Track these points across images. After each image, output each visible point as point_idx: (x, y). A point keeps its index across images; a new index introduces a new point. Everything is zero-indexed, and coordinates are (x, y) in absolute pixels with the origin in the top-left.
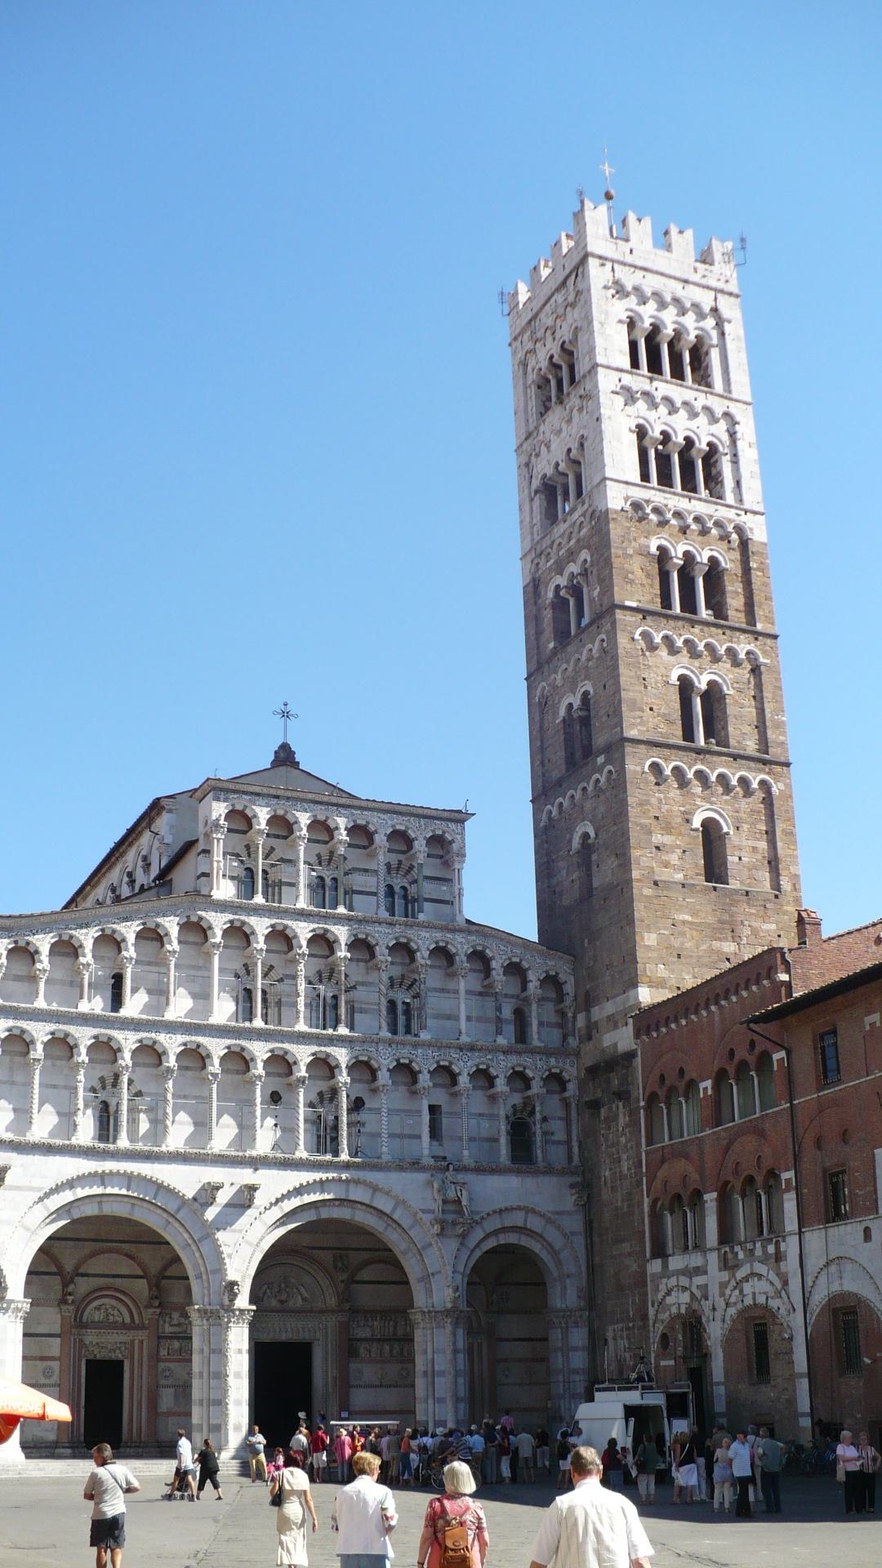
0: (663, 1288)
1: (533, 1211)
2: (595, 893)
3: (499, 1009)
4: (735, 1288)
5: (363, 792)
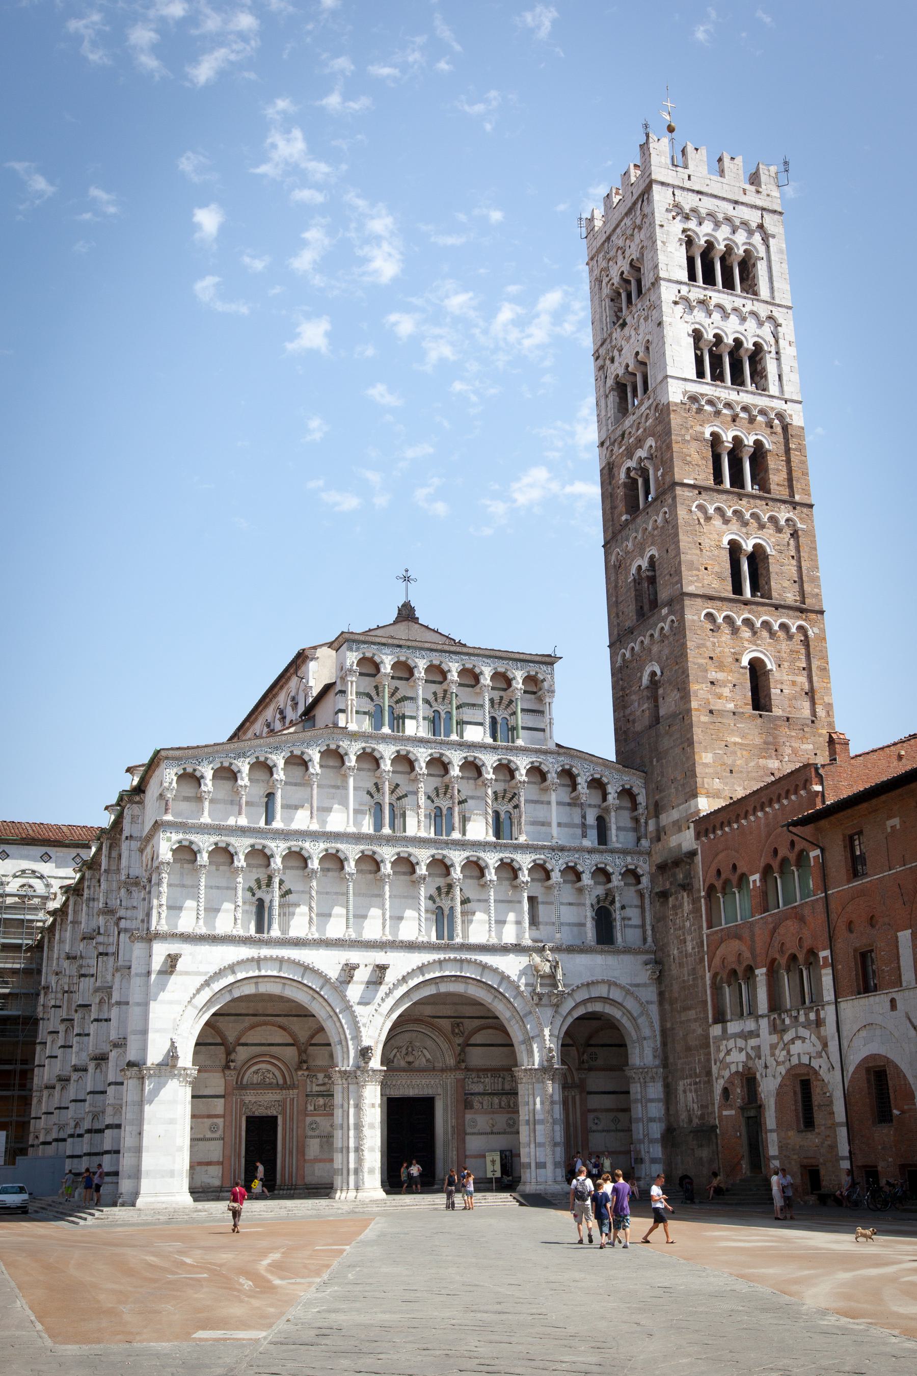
1: (615, 984)
3: (584, 817)
4: (783, 1050)
5: (471, 641)
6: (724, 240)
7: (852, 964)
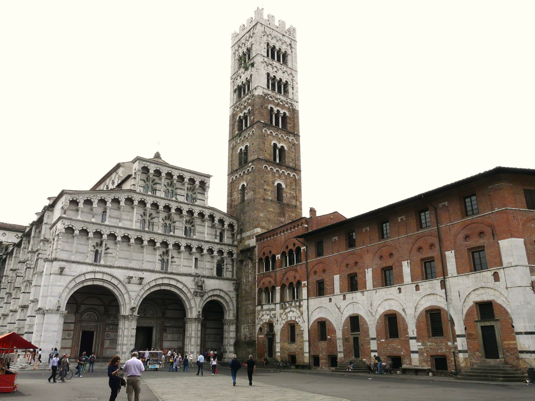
1: (222, 291)
3: (216, 232)
4: (285, 315)
7: (315, 286)
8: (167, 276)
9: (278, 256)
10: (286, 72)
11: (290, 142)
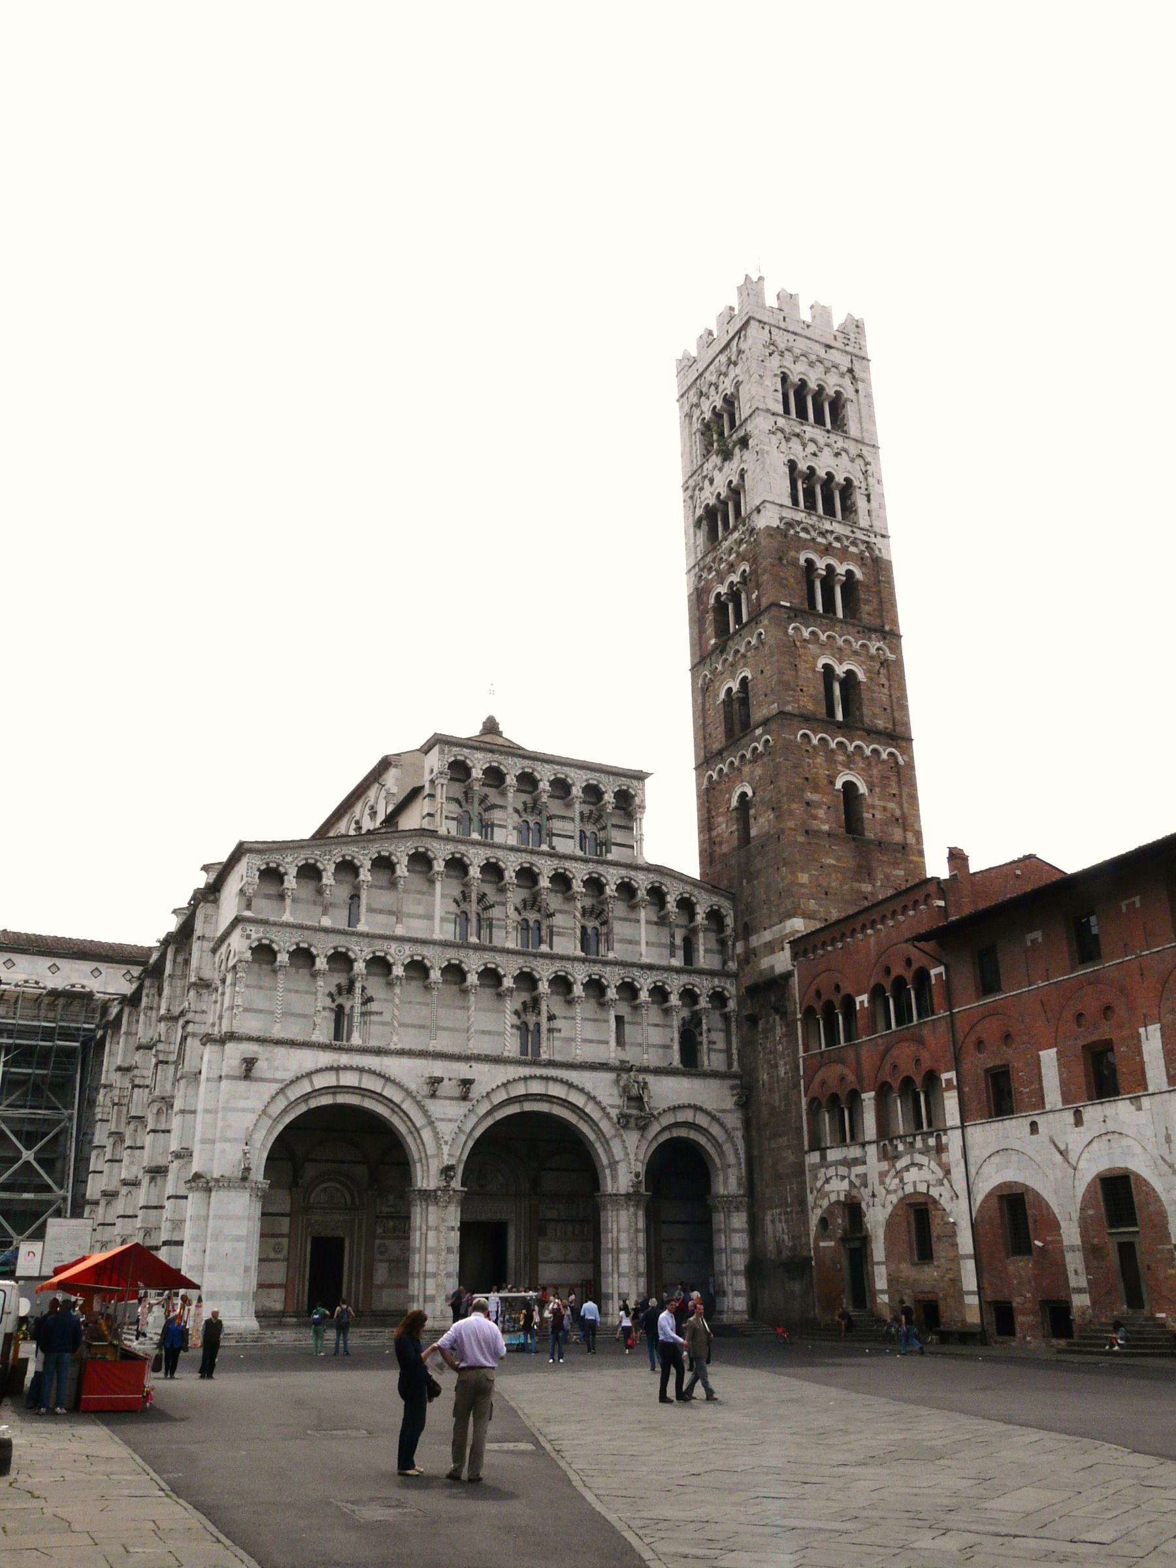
0: (821, 1175)
1: (701, 1109)
2: (751, 840)
3: (673, 936)
4: (895, 1177)
6: (817, 379)
8: (539, 1071)
9: (862, 999)
10: (846, 451)
11: (872, 658)
